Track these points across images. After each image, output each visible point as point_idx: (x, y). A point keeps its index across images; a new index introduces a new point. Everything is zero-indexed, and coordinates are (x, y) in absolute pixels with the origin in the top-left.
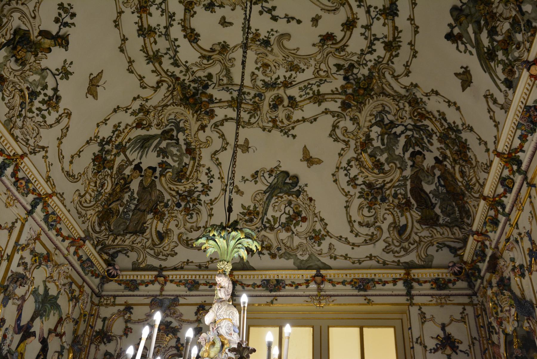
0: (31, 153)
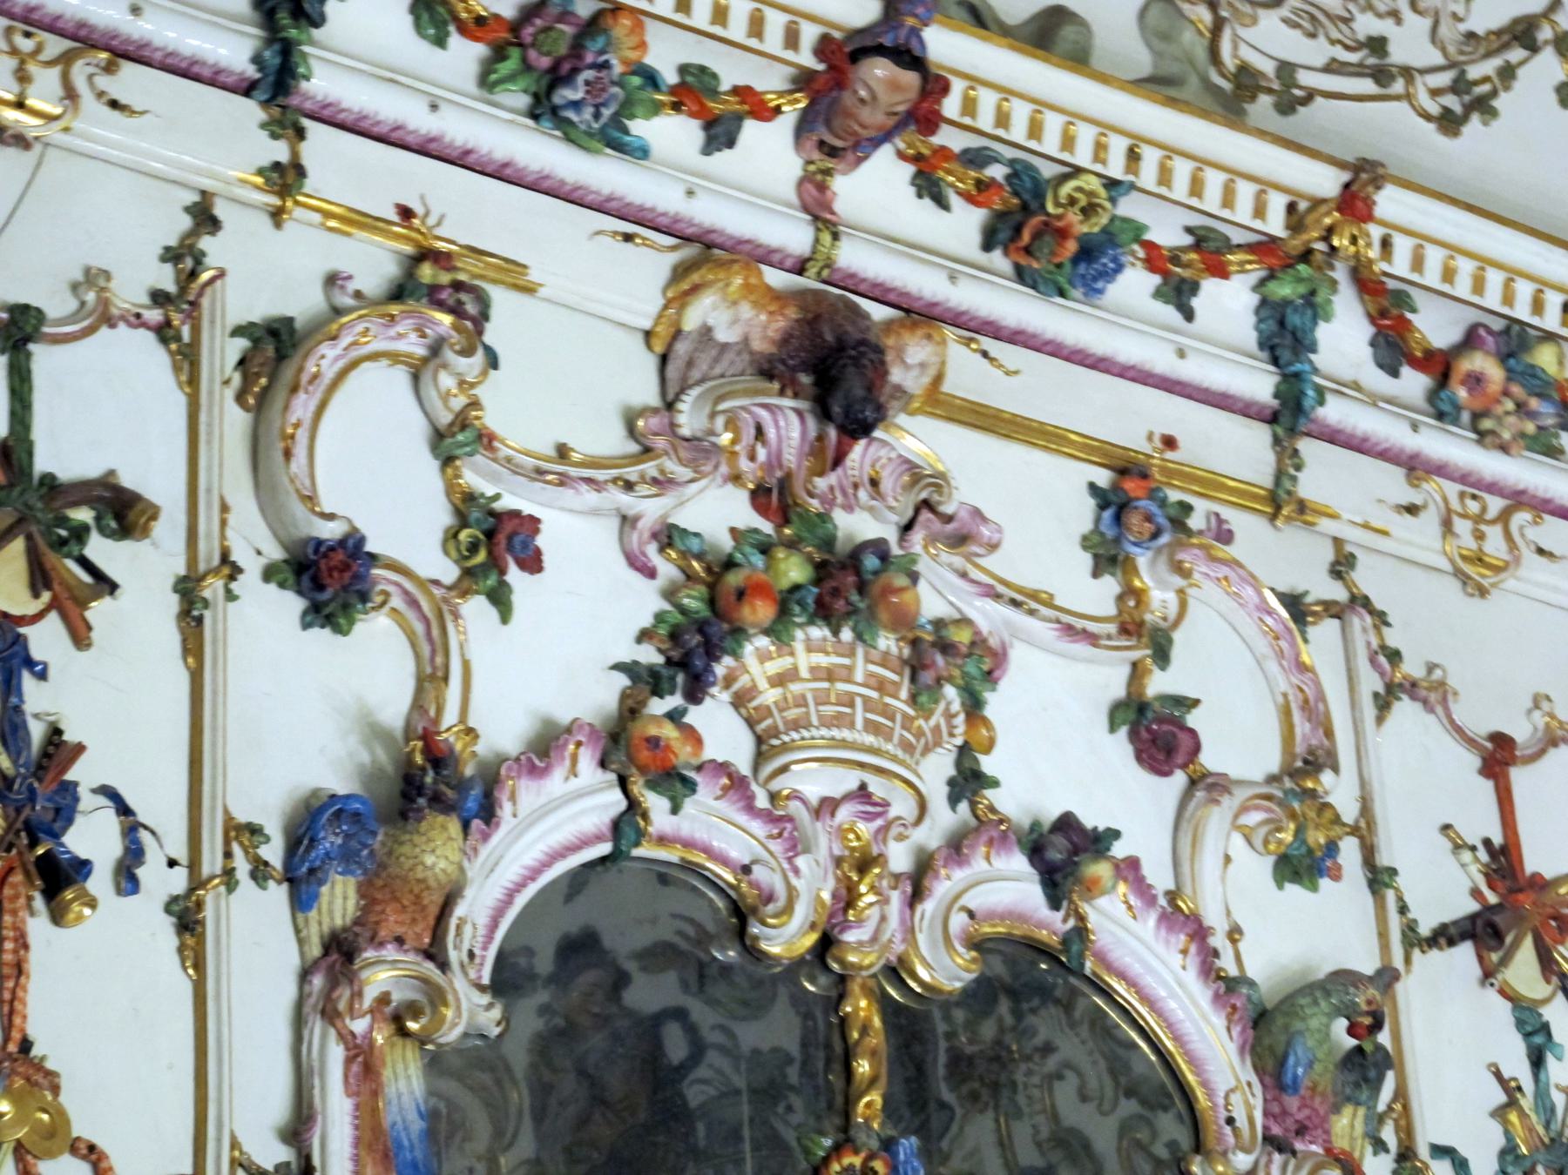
0: (1449, 123)
